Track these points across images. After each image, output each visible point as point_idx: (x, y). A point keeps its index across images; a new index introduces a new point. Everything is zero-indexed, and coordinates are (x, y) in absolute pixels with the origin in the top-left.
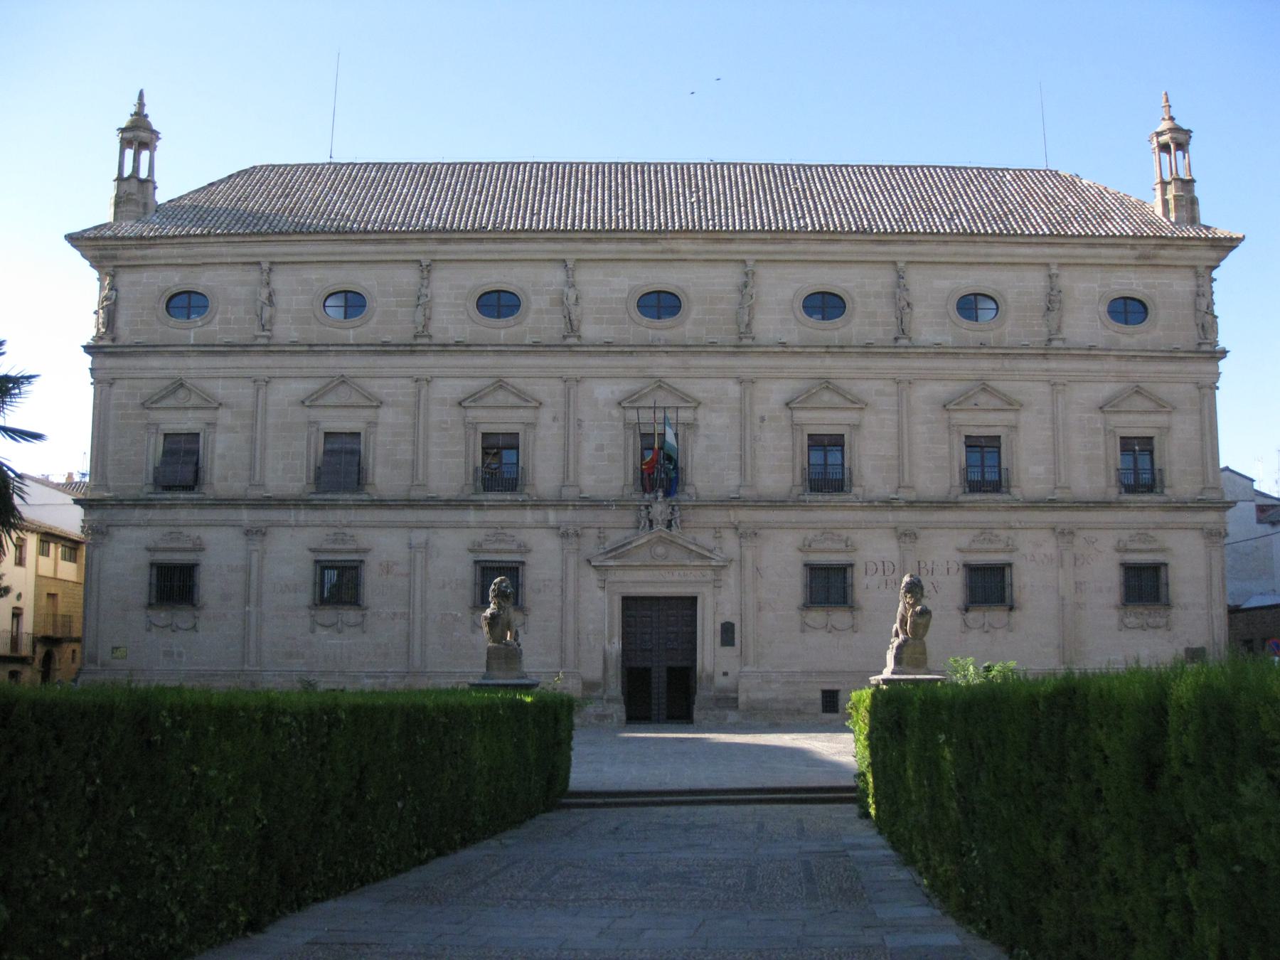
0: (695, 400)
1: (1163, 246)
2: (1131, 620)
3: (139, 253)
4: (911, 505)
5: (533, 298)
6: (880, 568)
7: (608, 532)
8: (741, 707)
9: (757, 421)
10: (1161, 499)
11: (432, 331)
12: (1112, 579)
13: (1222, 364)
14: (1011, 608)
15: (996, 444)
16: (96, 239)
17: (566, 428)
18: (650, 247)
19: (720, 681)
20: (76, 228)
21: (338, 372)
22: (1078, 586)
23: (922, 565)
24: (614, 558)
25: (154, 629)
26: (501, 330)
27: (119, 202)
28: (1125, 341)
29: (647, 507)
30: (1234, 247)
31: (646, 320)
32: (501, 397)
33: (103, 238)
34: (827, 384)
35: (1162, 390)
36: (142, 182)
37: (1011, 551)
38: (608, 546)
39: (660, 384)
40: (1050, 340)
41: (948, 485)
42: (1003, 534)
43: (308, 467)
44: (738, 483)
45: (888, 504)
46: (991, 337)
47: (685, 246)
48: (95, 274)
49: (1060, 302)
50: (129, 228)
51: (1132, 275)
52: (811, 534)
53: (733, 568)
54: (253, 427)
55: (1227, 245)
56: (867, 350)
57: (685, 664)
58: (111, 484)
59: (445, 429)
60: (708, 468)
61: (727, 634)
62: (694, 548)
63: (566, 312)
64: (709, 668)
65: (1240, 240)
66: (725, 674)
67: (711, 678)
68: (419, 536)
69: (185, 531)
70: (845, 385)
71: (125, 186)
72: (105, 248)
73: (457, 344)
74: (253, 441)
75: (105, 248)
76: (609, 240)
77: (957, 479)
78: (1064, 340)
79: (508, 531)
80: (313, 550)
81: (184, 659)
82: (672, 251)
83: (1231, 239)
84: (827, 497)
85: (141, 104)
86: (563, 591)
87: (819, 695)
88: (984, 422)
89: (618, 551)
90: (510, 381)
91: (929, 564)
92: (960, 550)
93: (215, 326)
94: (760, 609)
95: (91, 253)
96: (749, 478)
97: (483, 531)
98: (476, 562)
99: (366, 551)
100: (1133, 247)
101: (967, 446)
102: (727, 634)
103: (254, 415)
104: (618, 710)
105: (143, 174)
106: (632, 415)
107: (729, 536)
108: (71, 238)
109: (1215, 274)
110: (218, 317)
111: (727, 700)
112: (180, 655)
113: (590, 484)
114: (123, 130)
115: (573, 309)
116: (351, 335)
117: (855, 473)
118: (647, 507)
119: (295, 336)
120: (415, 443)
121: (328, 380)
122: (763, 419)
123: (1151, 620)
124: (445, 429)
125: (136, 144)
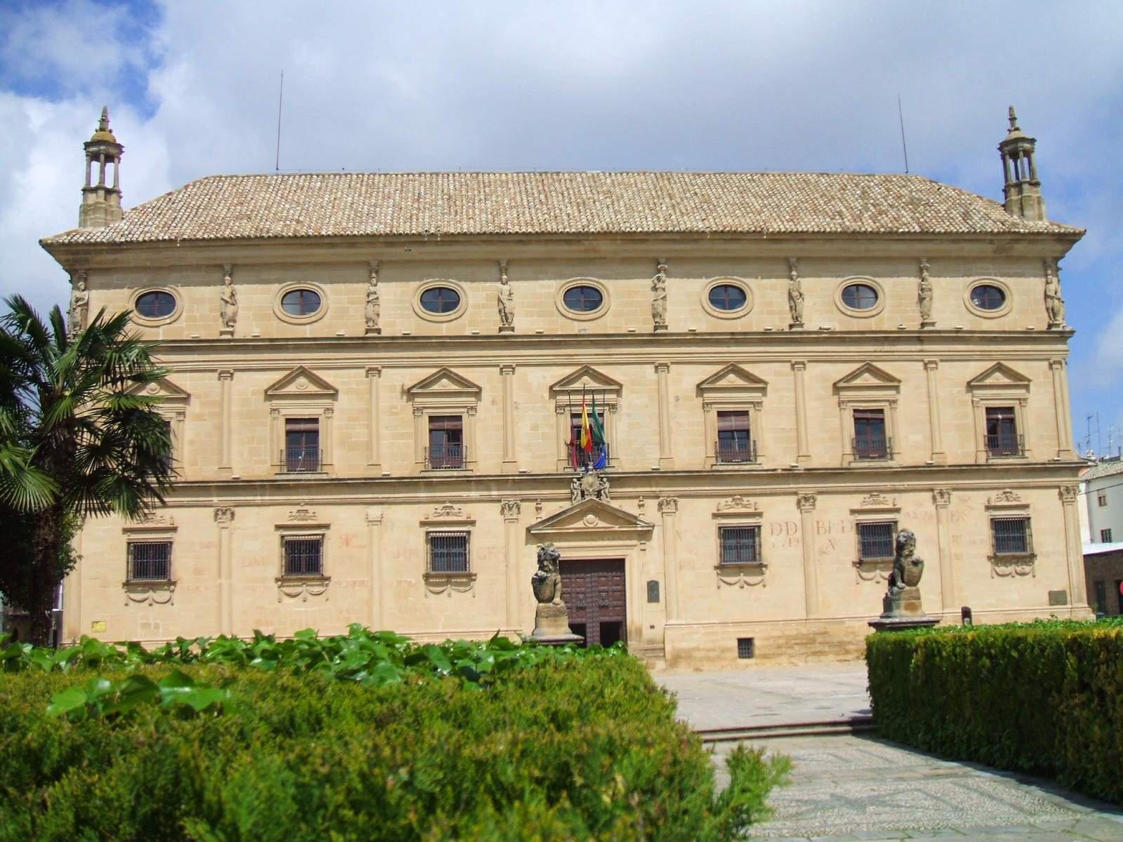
0: (616, 383)
1: (1017, 241)
2: (1002, 569)
3: (111, 257)
4: (813, 474)
5: (470, 294)
6: (784, 528)
7: (544, 504)
8: (668, 656)
9: (671, 399)
10: (1023, 461)
11: (380, 326)
12: (985, 534)
13: (1069, 341)
15: (880, 416)
16: (70, 244)
17: (504, 409)
18: (575, 247)
19: (647, 633)
20: (48, 236)
21: (297, 365)
22: (956, 538)
23: (821, 524)
24: (552, 525)
25: (132, 603)
26: (444, 325)
27: (85, 210)
28: (986, 325)
29: (579, 479)
30: (1075, 241)
31: (572, 313)
32: (445, 385)
33: (77, 244)
34: (735, 369)
35: (1019, 367)
36: (109, 192)
37: (898, 510)
38: (544, 515)
39: (587, 371)
40: (923, 325)
41: (840, 454)
42: (889, 497)
43: (272, 452)
44: (658, 456)
45: (790, 475)
46: (872, 325)
47: (605, 247)
48: (68, 277)
49: (930, 290)
50: (99, 233)
51: (991, 266)
52: (723, 501)
53: (656, 532)
54: (220, 414)
55: (1069, 239)
56: (767, 338)
57: (615, 619)
59: (395, 414)
60: (630, 445)
61: (653, 591)
62: (621, 515)
63: (502, 307)
65: (1081, 234)
66: (652, 627)
67: (639, 632)
68: (375, 511)
70: (746, 367)
71: (92, 198)
72: (77, 253)
73: (406, 337)
74: (220, 428)
75: (77, 253)
76: (539, 242)
77: (848, 450)
78: (933, 324)
79: (456, 506)
80: (278, 527)
81: (161, 630)
82: (594, 251)
83: (1074, 234)
84: (736, 468)
85: (104, 121)
86: (506, 556)
87: (736, 643)
88: (871, 399)
89: (553, 520)
90: (452, 370)
92: (853, 512)
93: (182, 323)
94: (681, 568)
95: (63, 257)
96: (667, 450)
97: (432, 506)
98: (428, 533)
99: (327, 526)
100: (991, 242)
101: (856, 420)
102: (653, 591)
103: (221, 402)
105: (109, 184)
106: (563, 399)
107: (652, 504)
108: (45, 245)
109: (1060, 264)
110: (184, 315)
112: (157, 626)
113: (527, 463)
114: (87, 145)
115: (507, 303)
116: (308, 332)
117: (759, 445)
118: (579, 479)
119: (256, 331)
120: (369, 427)
121: (288, 372)
122: (677, 399)
123: (1019, 569)
124: (395, 414)
125: (102, 157)
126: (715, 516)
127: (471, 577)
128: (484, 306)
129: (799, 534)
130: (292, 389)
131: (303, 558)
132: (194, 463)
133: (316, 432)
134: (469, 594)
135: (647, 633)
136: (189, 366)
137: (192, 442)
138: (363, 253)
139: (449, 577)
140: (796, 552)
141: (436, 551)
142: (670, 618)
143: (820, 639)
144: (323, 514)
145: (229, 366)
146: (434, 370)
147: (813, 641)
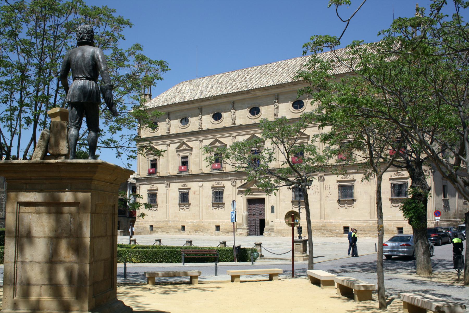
14: (354, 201)
18: (250, 95)
37: (354, 181)
38: (243, 183)
42: (351, 176)
47: (258, 93)
58: (141, 174)
61: (273, 208)
64: (268, 220)
68: (201, 184)
69: (155, 185)
80: (180, 189)
91: (328, 186)
98: (213, 190)
99: (190, 189)
102: (273, 208)
104: (245, 232)
111: (272, 229)
126: (212, 187)
127: (224, 204)
128: (228, 117)
129: (319, 190)
130: (182, 148)
131: (184, 198)
132: (162, 171)
133: (188, 161)
134: (223, 209)
135: (271, 223)
136: (160, 143)
137: (161, 165)
138: (196, 105)
139: (218, 204)
140: (318, 196)
141: (217, 196)
142: (277, 218)
143: (323, 228)
144: (189, 185)
145: (168, 143)
146: (214, 140)
147: (321, 229)
